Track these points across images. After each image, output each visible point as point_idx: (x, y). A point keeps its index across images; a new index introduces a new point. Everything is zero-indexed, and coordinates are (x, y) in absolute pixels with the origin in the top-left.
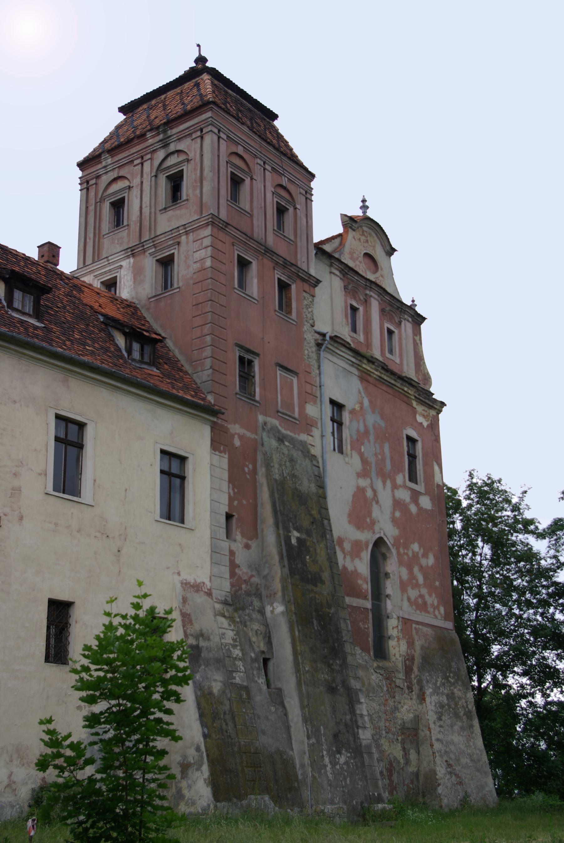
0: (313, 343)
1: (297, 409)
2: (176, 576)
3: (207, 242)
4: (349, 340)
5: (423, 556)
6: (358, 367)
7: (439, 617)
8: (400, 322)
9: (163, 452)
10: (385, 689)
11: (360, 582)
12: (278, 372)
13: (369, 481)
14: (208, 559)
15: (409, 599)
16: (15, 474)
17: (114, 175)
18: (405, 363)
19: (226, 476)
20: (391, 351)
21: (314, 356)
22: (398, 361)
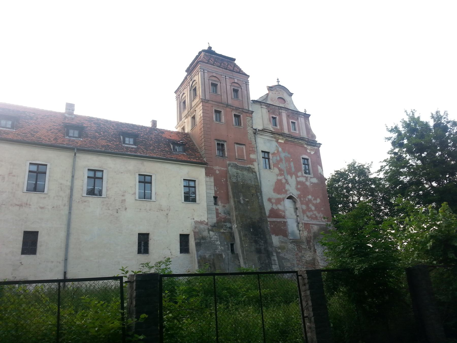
0: (252, 133)
1: (245, 157)
2: (193, 220)
3: (201, 108)
4: (272, 129)
5: (314, 200)
6: (275, 138)
8: (298, 119)
9: (184, 180)
10: (296, 249)
11: (280, 212)
12: (236, 146)
13: (283, 177)
14: (206, 213)
15: (307, 216)
16: (123, 196)
17: (182, 93)
18: (301, 132)
19: (213, 184)
20: (295, 130)
21: (253, 137)
22: (297, 132)
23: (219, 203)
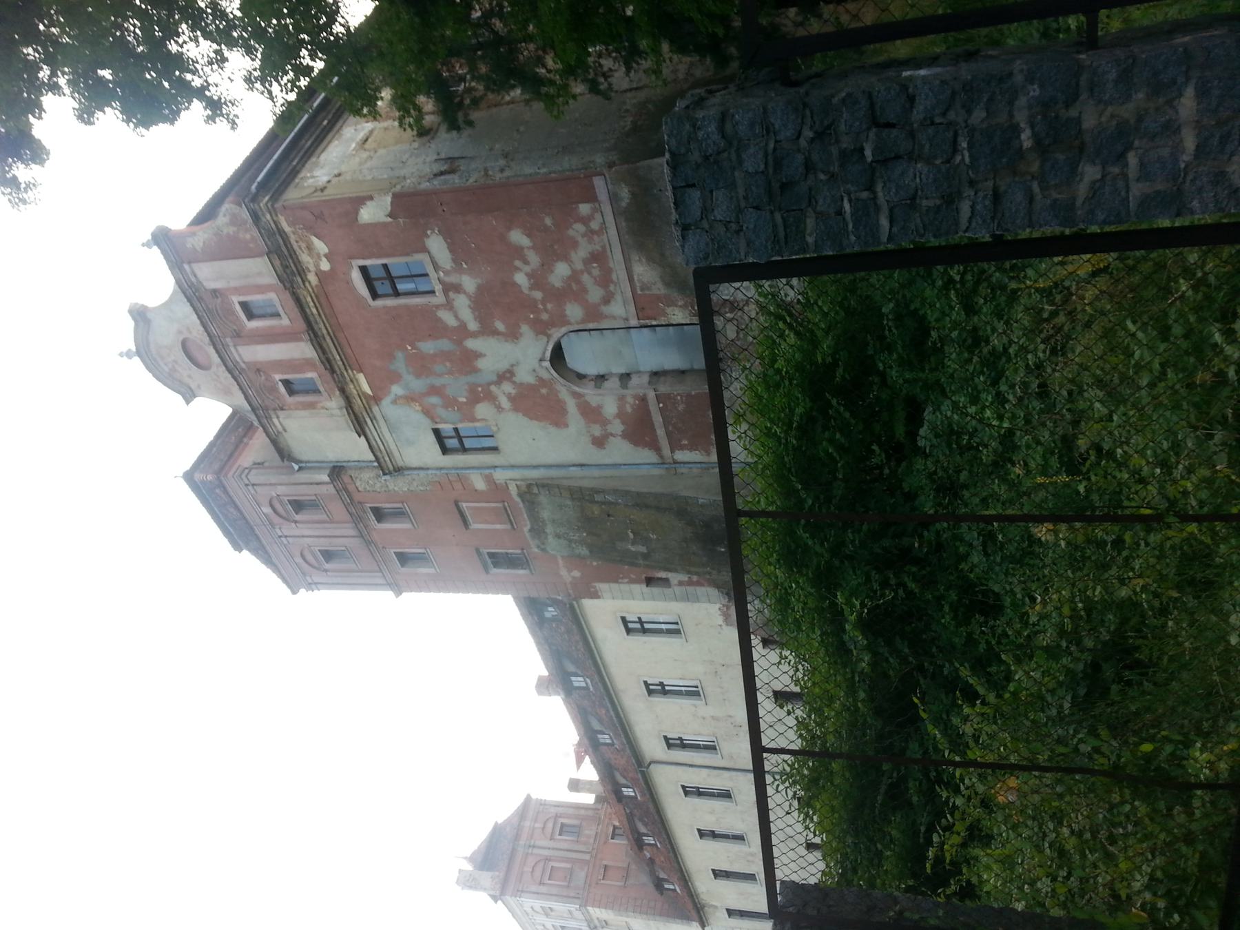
5: (526, 262)
6: (369, 411)
7: (598, 216)
11: (629, 410)
15: (607, 300)
23: (662, 575)
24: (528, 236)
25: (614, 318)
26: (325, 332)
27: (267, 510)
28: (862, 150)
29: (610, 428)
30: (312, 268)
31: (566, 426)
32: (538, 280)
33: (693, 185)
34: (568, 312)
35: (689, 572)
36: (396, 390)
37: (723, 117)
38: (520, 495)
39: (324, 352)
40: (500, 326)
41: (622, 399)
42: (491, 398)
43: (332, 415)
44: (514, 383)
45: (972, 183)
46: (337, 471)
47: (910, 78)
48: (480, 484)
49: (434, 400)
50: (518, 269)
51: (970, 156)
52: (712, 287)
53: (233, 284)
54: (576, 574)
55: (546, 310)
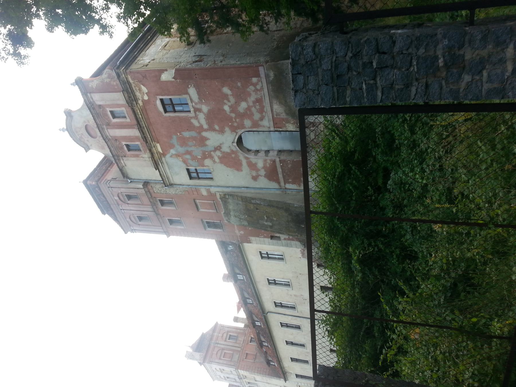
5: (229, 101)
6: (160, 159)
7: (260, 83)
11: (268, 166)
15: (262, 119)
23: (278, 235)
24: (231, 90)
25: (264, 126)
26: (144, 125)
27: (117, 198)
28: (372, 63)
29: (260, 173)
30: (141, 99)
31: (242, 171)
32: (233, 109)
33: (300, 74)
34: (245, 123)
35: (289, 235)
36: (172, 151)
37: (315, 46)
38: (221, 198)
39: (143, 134)
40: (217, 127)
41: (265, 161)
42: (211, 157)
43: (145, 160)
44: (221, 151)
45: (417, 80)
46: (146, 184)
47: (394, 34)
48: (205, 193)
49: (188, 157)
50: (225, 104)
51: (417, 68)
52: (306, 117)
53: (108, 103)
54: (242, 232)
55: (236, 121)
